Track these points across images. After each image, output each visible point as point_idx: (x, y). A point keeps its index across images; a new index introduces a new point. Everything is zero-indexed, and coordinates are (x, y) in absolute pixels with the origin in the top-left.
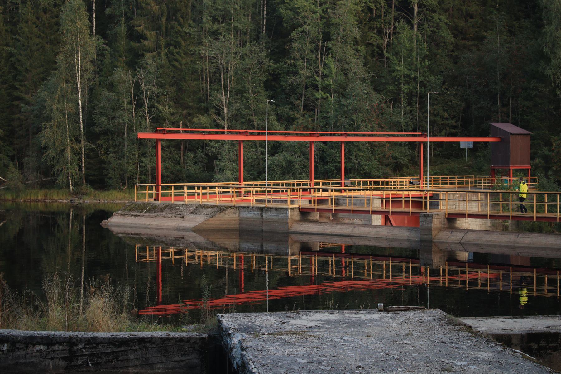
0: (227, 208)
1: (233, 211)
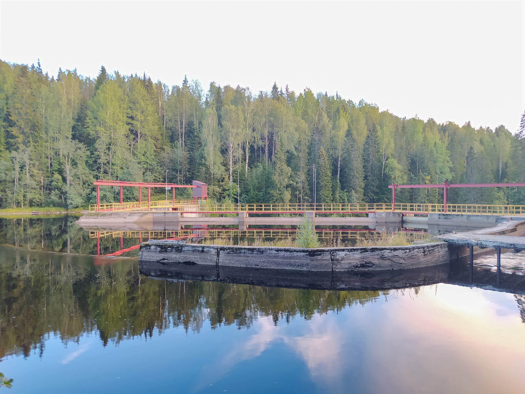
0: (148, 213)
1: (150, 214)
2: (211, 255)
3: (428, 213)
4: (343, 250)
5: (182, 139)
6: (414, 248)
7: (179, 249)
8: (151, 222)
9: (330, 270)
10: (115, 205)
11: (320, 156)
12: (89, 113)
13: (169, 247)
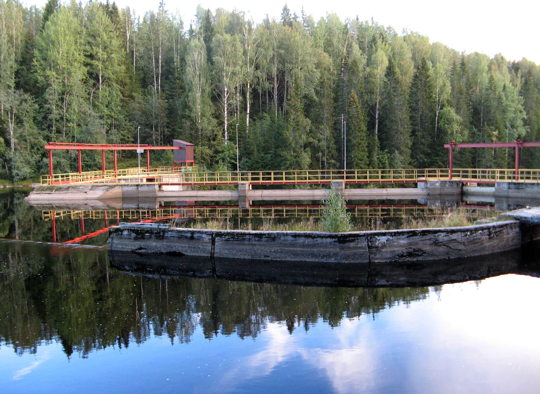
0: (115, 186)
2: (203, 243)
3: (495, 182)
4: (384, 234)
5: (157, 83)
6: (476, 230)
7: (160, 235)
8: (119, 198)
9: (367, 261)
10: (72, 176)
11: (350, 103)
12: (36, 52)
13: (147, 232)
